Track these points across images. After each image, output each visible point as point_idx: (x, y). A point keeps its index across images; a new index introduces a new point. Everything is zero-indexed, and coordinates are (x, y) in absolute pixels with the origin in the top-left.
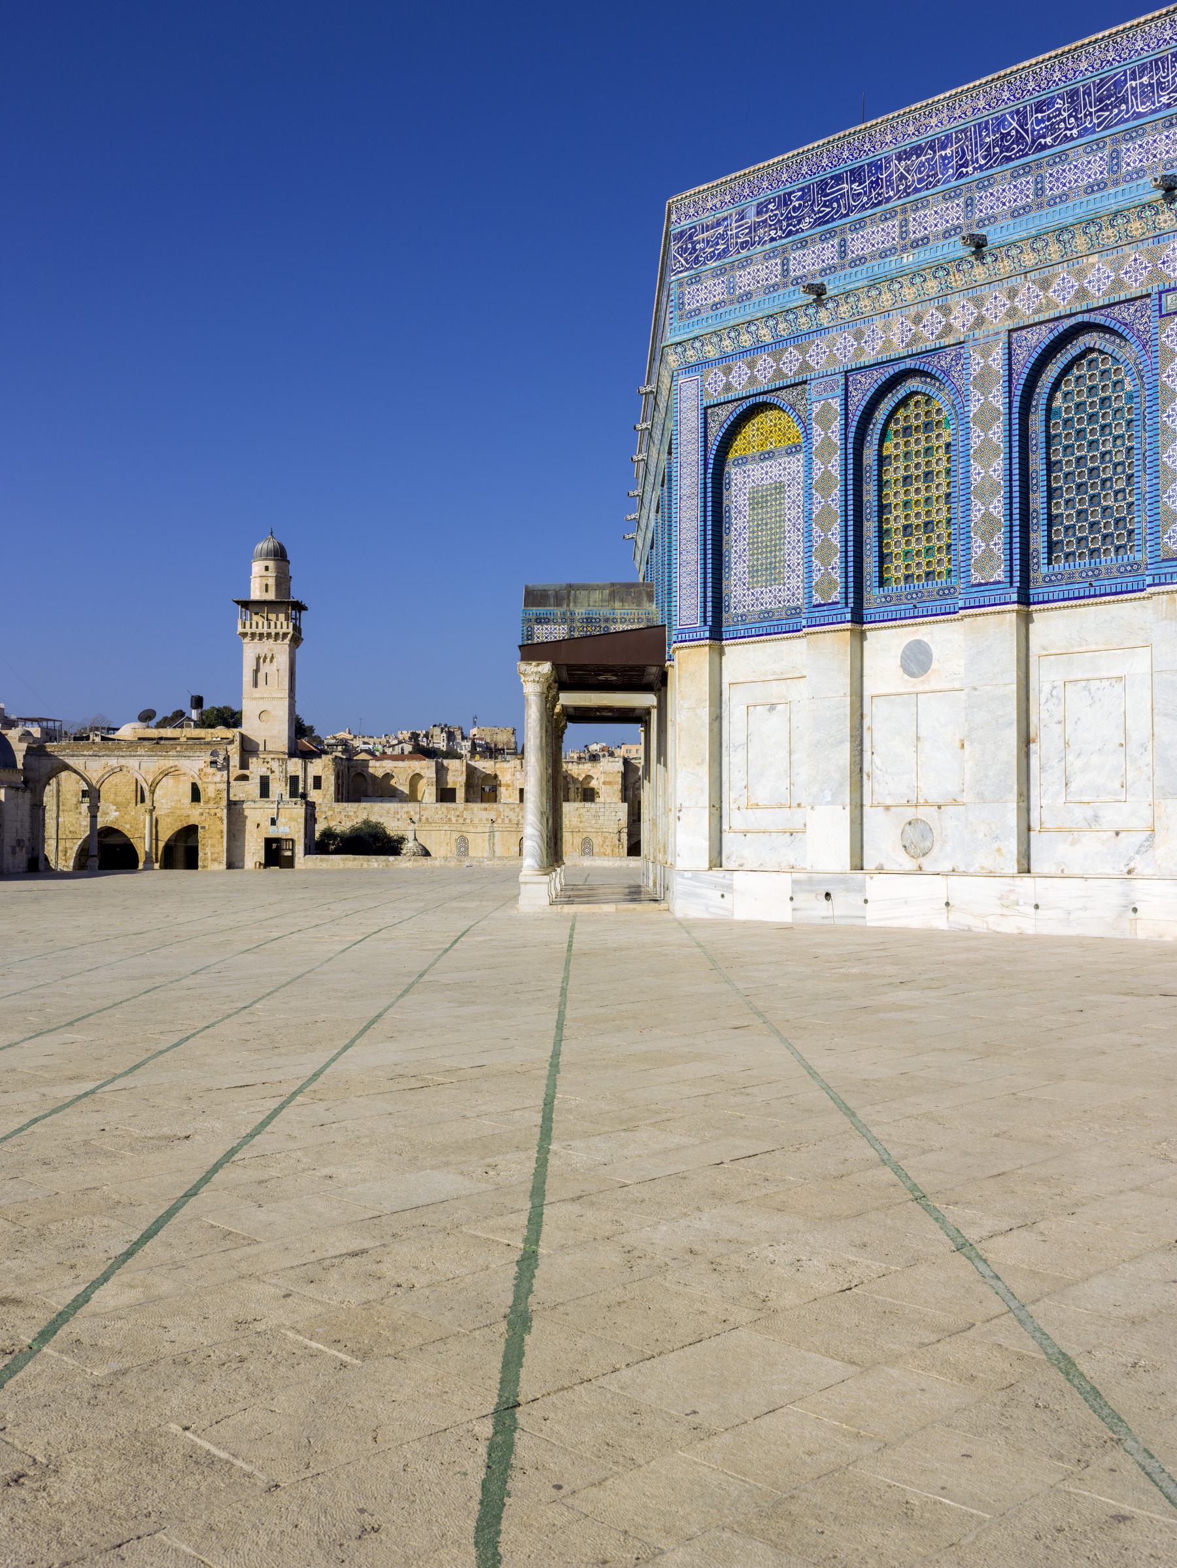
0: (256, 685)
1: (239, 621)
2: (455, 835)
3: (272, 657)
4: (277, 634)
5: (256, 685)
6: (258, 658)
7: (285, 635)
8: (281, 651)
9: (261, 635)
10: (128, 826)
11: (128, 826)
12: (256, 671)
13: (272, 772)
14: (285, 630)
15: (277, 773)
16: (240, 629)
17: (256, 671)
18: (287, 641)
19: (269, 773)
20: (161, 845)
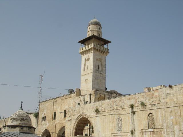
0: (84, 70)
1: (80, 49)
2: (116, 117)
3: (89, 58)
4: (89, 49)
5: (84, 70)
6: (85, 60)
7: (91, 48)
8: (91, 55)
9: (85, 51)
10: (50, 129)
11: (50, 129)
12: (85, 65)
13: (81, 101)
14: (91, 47)
15: (82, 101)
16: (80, 51)
17: (85, 65)
18: (92, 51)
19: (80, 102)
20: (56, 135)
